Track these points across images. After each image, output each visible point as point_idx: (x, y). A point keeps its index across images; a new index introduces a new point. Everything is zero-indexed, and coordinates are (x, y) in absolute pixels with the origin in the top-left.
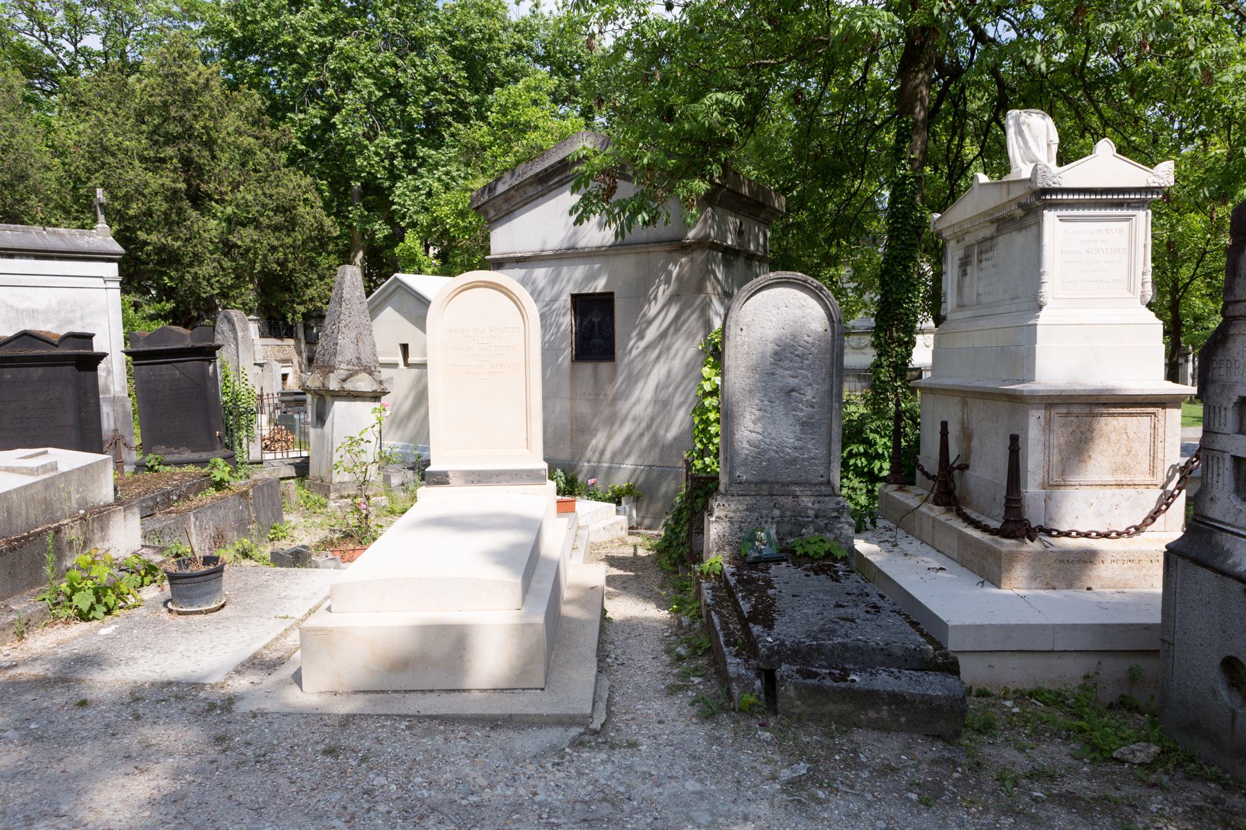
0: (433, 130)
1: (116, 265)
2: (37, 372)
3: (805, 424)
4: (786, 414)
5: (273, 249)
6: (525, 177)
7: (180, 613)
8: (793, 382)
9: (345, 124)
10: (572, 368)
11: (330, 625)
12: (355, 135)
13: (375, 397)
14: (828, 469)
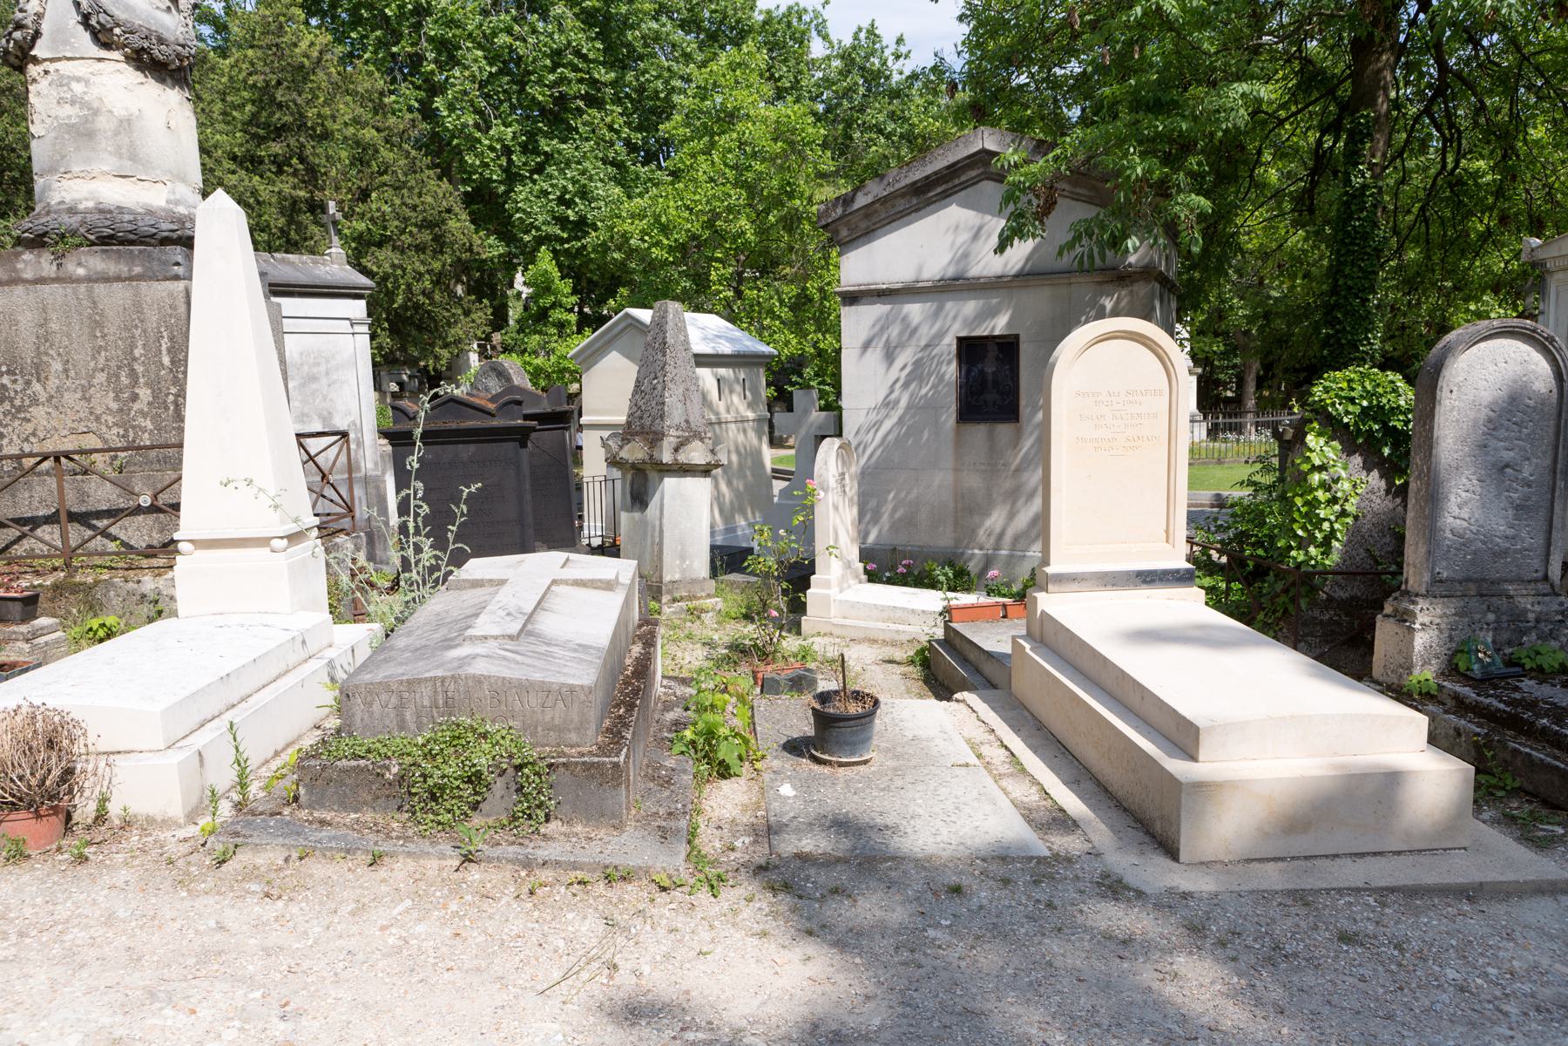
0: (558, 117)
1: (363, 303)
2: (467, 451)
3: (1521, 508)
4: (1498, 496)
5: (419, 276)
6: (898, 186)
7: (841, 765)
8: (1508, 456)
9: (451, 108)
10: (958, 432)
11: (1218, 778)
12: (465, 126)
13: (705, 471)
14: (1547, 562)
